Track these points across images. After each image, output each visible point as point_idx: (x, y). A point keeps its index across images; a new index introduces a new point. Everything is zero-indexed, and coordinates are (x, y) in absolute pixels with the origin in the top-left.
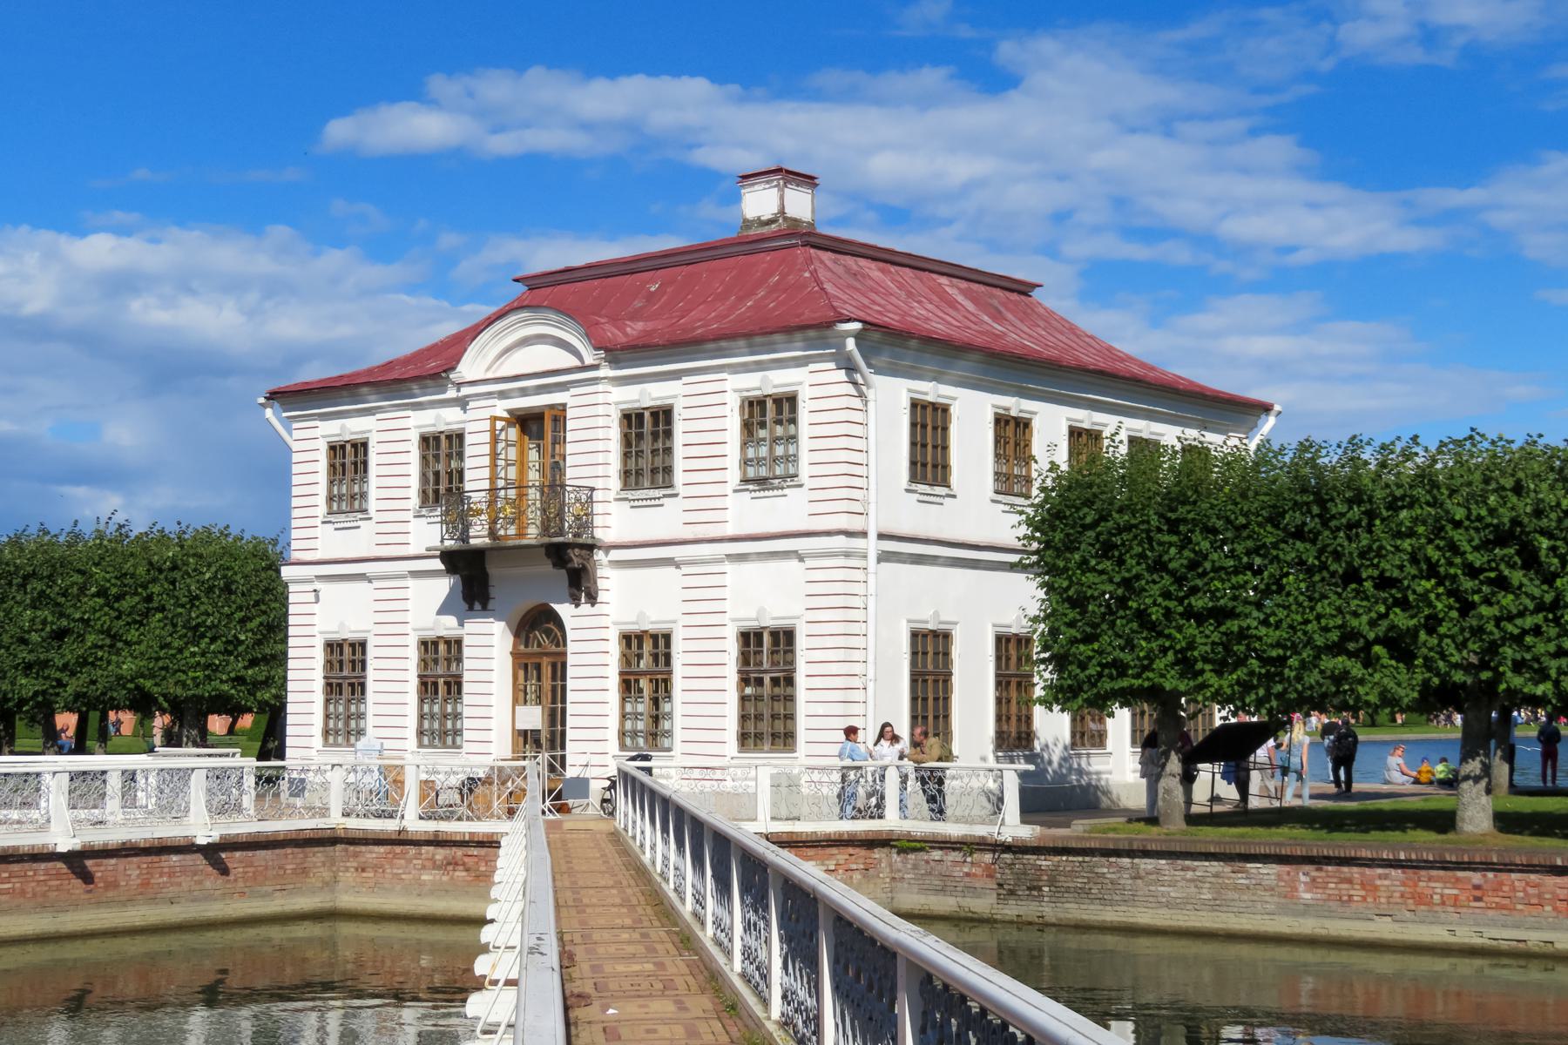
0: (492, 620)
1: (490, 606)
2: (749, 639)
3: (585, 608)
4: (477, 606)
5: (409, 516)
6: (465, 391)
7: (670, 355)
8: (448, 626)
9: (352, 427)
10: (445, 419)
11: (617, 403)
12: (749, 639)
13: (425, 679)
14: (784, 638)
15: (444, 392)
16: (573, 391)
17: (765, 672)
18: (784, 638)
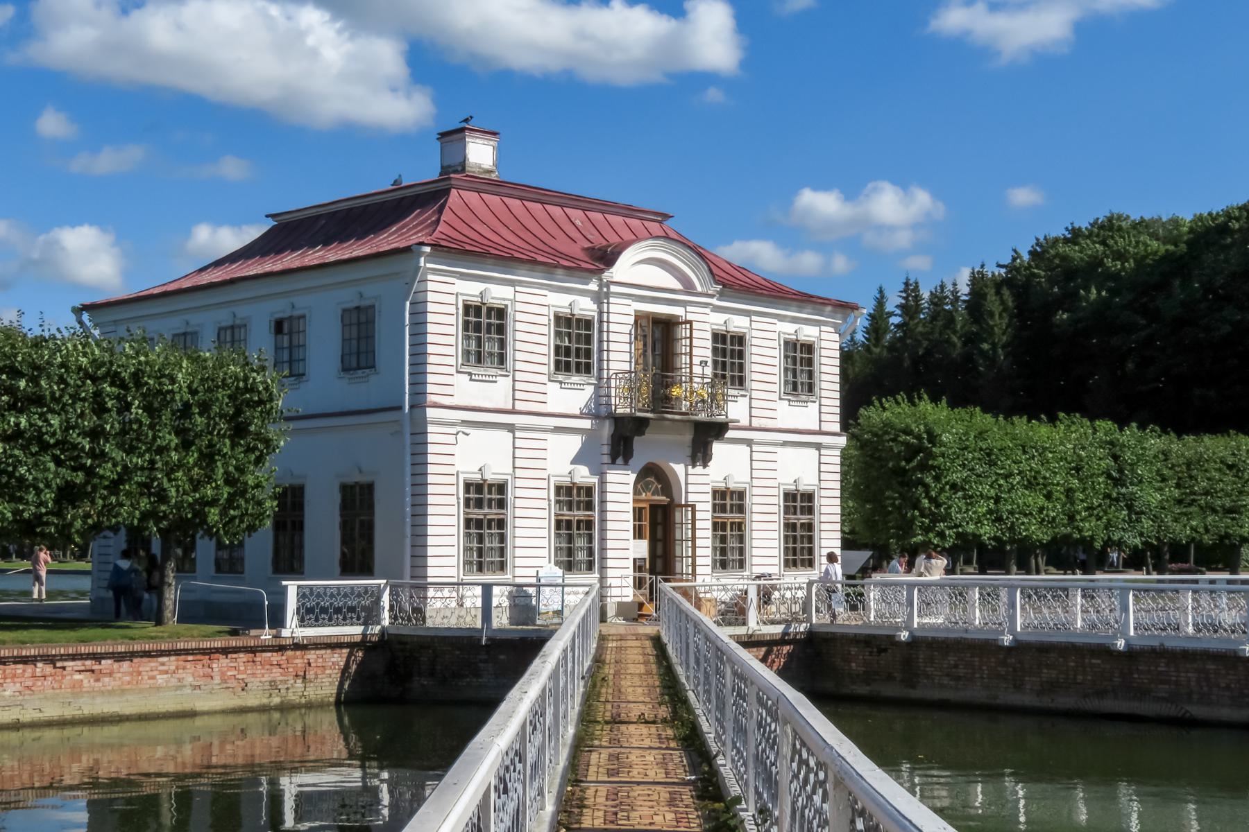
0: (629, 472)
1: (631, 462)
2: (790, 497)
3: (699, 469)
4: (620, 460)
5: (544, 379)
6: (613, 288)
7: (754, 300)
8: (583, 475)
9: (498, 294)
10: (585, 307)
11: (712, 324)
12: (790, 497)
13: (560, 518)
14: (809, 497)
15: (587, 284)
16: (689, 309)
17: (798, 519)
18: (809, 497)
